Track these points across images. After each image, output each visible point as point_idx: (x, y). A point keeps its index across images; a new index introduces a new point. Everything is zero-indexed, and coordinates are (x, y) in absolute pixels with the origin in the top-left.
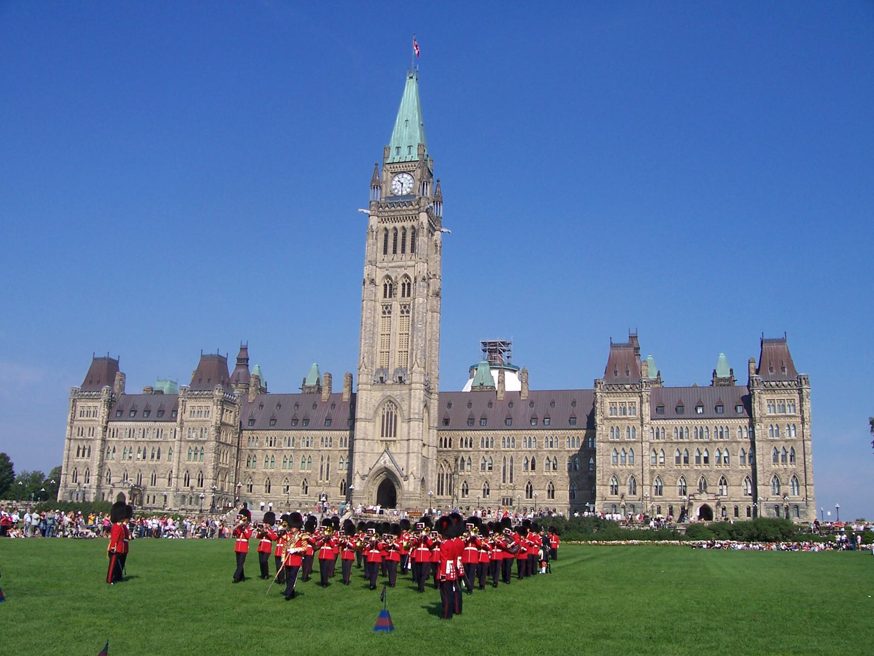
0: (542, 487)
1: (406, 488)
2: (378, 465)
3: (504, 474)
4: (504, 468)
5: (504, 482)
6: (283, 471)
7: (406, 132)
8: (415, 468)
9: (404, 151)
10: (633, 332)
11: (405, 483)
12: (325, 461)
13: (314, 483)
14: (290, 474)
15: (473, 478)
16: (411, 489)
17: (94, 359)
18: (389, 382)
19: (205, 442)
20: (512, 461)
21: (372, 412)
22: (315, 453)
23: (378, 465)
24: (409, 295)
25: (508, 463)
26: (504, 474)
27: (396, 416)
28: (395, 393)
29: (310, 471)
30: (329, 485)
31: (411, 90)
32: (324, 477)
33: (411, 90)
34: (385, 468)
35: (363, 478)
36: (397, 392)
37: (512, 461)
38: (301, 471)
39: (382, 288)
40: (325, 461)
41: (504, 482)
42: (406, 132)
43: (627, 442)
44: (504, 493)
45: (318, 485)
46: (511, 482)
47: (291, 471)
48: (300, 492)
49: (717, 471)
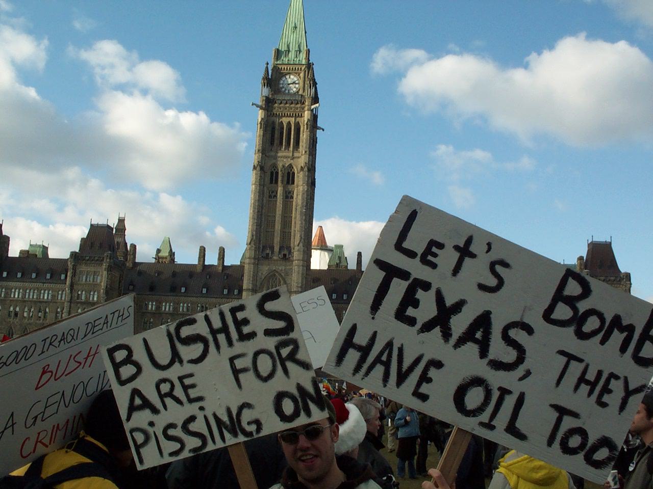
9: (292, 55)
18: (275, 258)
21: (258, 284)
24: (293, 183)
36: (281, 268)
39: (269, 174)
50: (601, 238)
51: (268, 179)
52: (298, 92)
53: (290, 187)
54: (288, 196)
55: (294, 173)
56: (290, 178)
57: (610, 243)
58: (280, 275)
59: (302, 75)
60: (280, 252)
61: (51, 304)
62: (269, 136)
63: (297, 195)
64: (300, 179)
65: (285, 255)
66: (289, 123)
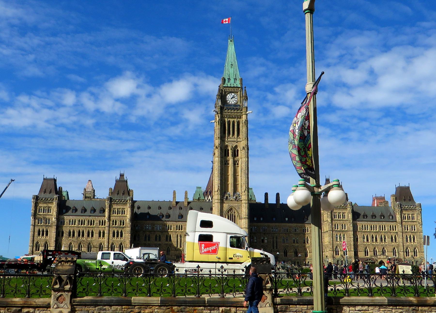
0: (292, 251)
3: (273, 245)
5: (273, 248)
7: (231, 71)
9: (232, 81)
10: (327, 177)
12: (179, 237)
17: (44, 179)
19: (123, 228)
20: (277, 238)
22: (174, 233)
24: (238, 156)
25: (275, 239)
26: (273, 245)
27: (235, 216)
28: (235, 205)
31: (231, 48)
33: (231, 48)
36: (235, 204)
37: (277, 238)
38: (166, 243)
40: (179, 237)
41: (273, 248)
42: (231, 71)
43: (343, 231)
46: (277, 248)
49: (382, 245)
50: (403, 184)
51: (224, 154)
52: (237, 103)
53: (236, 159)
54: (235, 163)
55: (238, 150)
56: (235, 153)
57: (408, 188)
58: (235, 209)
59: (239, 93)
60: (234, 196)
61: (95, 228)
62: (222, 128)
63: (241, 163)
64: (242, 154)
65: (236, 197)
66: (234, 122)
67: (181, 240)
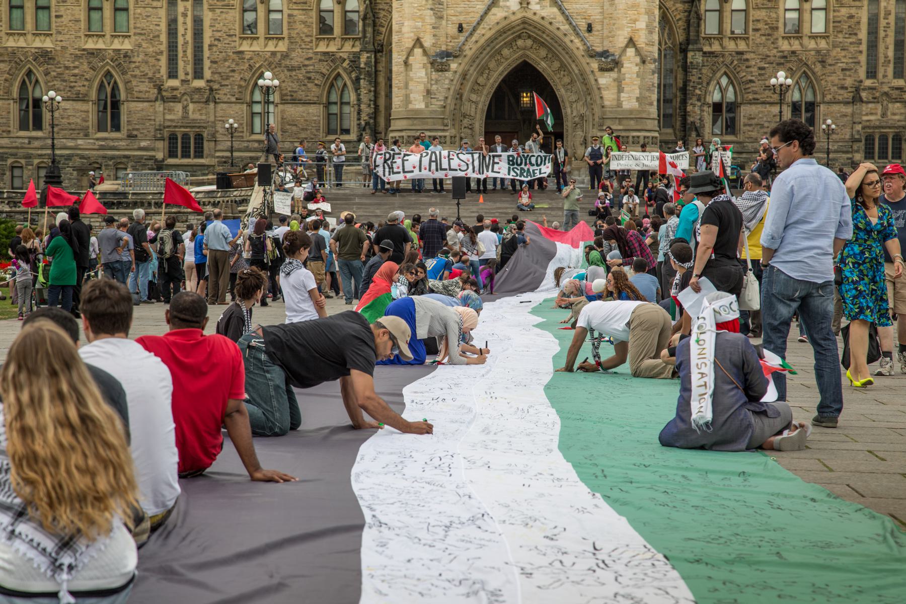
1: (609, 97)
2: (497, 14)
3: (873, 46)
4: (873, 22)
5: (872, 73)
6: (11, 43)
8: (642, 24)
11: (605, 80)
13: (144, 87)
14: (45, 56)
15: (755, 61)
16: (629, 102)
23: (497, 14)
26: (873, 46)
29: (127, 45)
30: (210, 97)
32: (185, 66)
34: (525, 22)
35: (440, 61)
38: (90, 45)
41: (872, 73)
44: (871, 114)
45: (164, 96)
47: (48, 44)
48: (92, 118)
67: (198, 22)
